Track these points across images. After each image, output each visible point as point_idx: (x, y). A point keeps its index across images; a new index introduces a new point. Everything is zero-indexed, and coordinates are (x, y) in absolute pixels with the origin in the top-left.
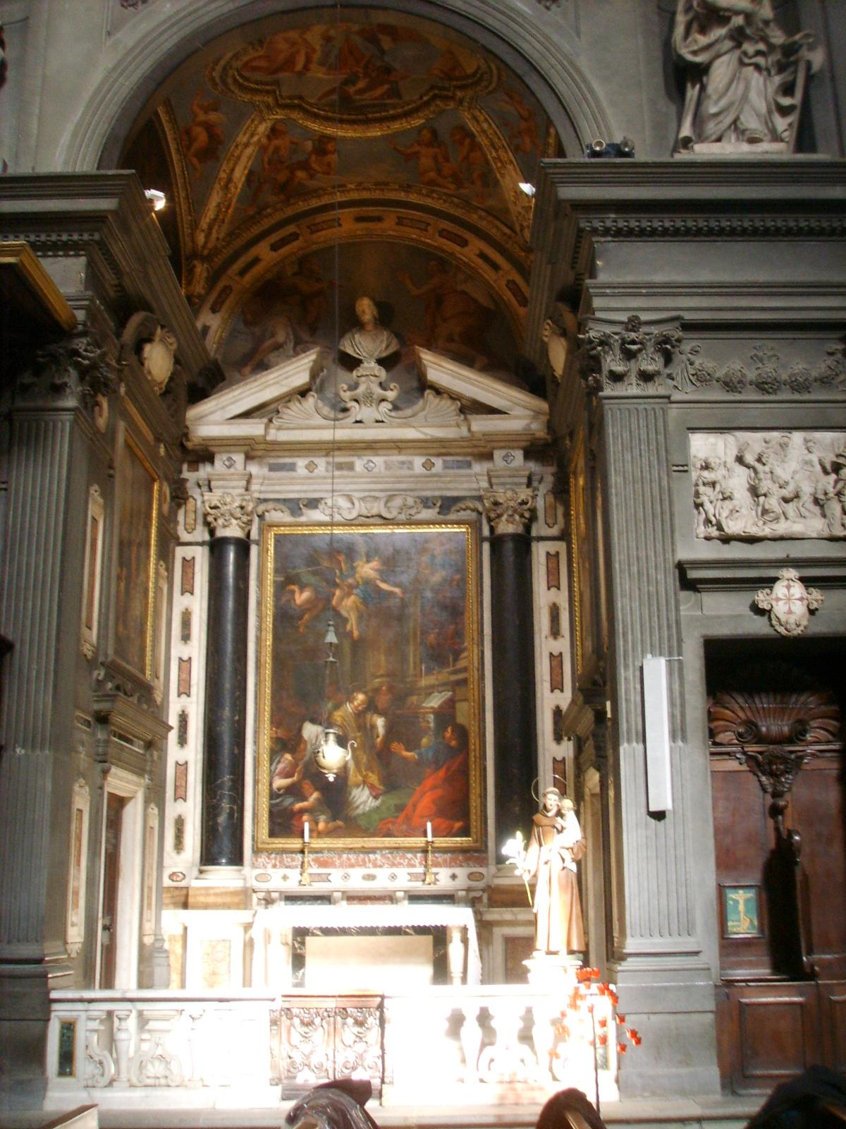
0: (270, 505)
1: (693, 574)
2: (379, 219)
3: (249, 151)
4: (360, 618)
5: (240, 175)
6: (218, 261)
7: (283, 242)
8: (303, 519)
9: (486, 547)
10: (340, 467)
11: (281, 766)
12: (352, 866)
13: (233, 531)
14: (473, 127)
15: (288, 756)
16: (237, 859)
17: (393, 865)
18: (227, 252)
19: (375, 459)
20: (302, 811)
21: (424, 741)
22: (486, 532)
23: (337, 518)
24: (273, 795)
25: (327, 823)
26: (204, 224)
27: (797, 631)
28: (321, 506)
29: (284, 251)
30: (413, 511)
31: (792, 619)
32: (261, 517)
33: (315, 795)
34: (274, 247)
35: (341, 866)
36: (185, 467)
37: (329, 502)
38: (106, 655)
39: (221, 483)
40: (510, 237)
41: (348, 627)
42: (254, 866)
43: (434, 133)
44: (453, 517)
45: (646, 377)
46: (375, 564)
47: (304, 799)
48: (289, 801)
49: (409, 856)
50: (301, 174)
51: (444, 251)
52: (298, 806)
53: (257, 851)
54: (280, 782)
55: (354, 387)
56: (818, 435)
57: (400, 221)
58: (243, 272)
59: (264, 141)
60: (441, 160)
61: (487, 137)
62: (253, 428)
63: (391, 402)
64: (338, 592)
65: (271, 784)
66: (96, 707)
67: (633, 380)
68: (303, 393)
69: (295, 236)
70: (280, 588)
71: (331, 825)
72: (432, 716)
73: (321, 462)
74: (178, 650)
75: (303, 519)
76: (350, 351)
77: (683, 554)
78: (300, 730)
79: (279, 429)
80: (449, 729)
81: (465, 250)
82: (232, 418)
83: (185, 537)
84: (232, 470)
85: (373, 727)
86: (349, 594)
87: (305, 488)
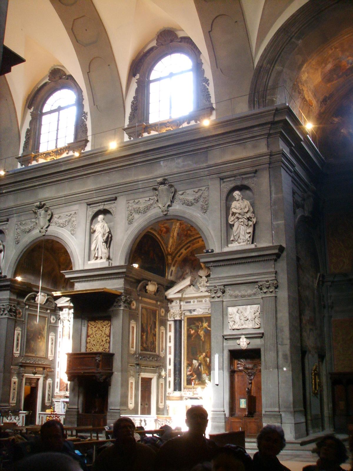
0: (185, 311)
1: (225, 337)
3: (176, 229)
5: (175, 234)
6: (173, 255)
7: (188, 248)
8: (192, 314)
10: (200, 301)
11: (189, 370)
13: (178, 318)
15: (190, 367)
16: (180, 390)
18: (176, 252)
20: (193, 379)
24: (187, 376)
25: (198, 382)
26: (169, 246)
27: (245, 348)
28: (196, 311)
29: (188, 250)
31: (244, 346)
32: (184, 314)
33: (195, 376)
34: (185, 250)
36: (169, 303)
38: (138, 352)
39: (174, 307)
42: (184, 391)
45: (219, 297)
47: (193, 377)
48: (190, 377)
50: (189, 232)
52: (192, 378)
53: (184, 388)
54: (189, 373)
56: (253, 306)
58: (179, 257)
59: (179, 226)
62: (179, 295)
64: (199, 330)
66: (136, 362)
67: (216, 298)
68: (190, 286)
69: (189, 246)
70: (188, 330)
73: (196, 300)
74: (169, 344)
75: (192, 314)
77: (225, 333)
78: (192, 361)
79: (185, 294)
82: (175, 293)
83: (169, 319)
84: (177, 304)
85: (207, 361)
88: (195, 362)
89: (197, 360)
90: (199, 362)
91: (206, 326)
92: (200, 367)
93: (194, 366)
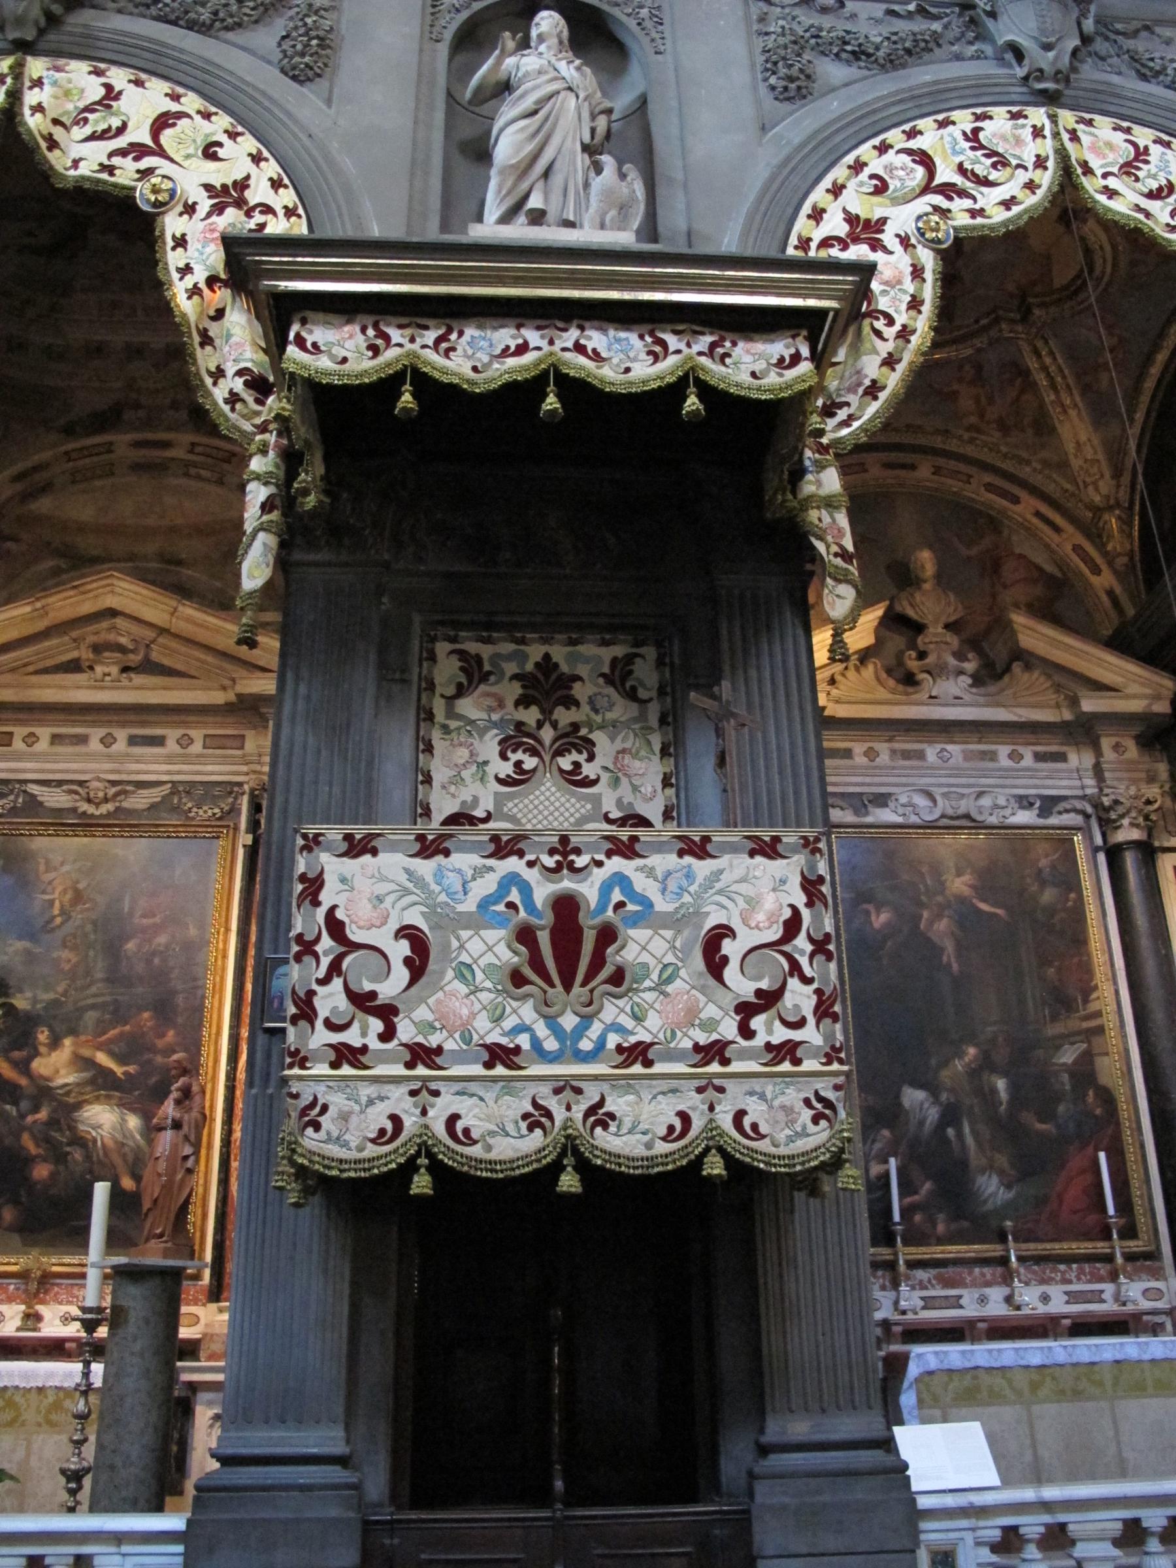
2: (913, 467)
4: (960, 947)
9: (1102, 858)
10: (906, 755)
11: (878, 1146)
12: (988, 1284)
14: (1032, 364)
15: (886, 1133)
17: (1043, 1281)
19: (949, 747)
21: (1061, 1108)
22: (1099, 841)
23: (914, 819)
28: (892, 804)
30: (1008, 812)
33: (928, 1186)
35: (974, 1284)
37: (903, 799)
40: (1073, 495)
41: (945, 959)
43: (979, 368)
44: (1053, 820)
46: (967, 878)
47: (916, 1193)
49: (1062, 1267)
51: (992, 508)
55: (922, 655)
57: (937, 471)
60: (983, 400)
61: (1048, 375)
63: (972, 676)
64: (926, 914)
65: (867, 1171)
71: (953, 1226)
72: (1065, 1077)
73: (883, 748)
75: (869, 819)
76: (911, 613)
78: (898, 1096)
80: (1091, 1093)
81: (1018, 508)
85: (994, 1091)
86: (939, 916)
87: (868, 780)
88: (913, 1097)
89: (933, 1089)
90: (944, 1097)
91: (967, 891)
92: (950, 1132)
93: (912, 1128)
